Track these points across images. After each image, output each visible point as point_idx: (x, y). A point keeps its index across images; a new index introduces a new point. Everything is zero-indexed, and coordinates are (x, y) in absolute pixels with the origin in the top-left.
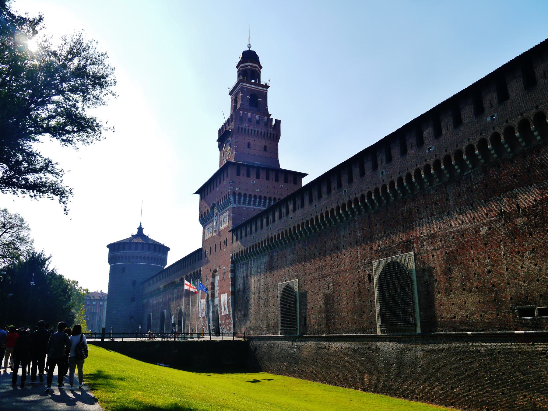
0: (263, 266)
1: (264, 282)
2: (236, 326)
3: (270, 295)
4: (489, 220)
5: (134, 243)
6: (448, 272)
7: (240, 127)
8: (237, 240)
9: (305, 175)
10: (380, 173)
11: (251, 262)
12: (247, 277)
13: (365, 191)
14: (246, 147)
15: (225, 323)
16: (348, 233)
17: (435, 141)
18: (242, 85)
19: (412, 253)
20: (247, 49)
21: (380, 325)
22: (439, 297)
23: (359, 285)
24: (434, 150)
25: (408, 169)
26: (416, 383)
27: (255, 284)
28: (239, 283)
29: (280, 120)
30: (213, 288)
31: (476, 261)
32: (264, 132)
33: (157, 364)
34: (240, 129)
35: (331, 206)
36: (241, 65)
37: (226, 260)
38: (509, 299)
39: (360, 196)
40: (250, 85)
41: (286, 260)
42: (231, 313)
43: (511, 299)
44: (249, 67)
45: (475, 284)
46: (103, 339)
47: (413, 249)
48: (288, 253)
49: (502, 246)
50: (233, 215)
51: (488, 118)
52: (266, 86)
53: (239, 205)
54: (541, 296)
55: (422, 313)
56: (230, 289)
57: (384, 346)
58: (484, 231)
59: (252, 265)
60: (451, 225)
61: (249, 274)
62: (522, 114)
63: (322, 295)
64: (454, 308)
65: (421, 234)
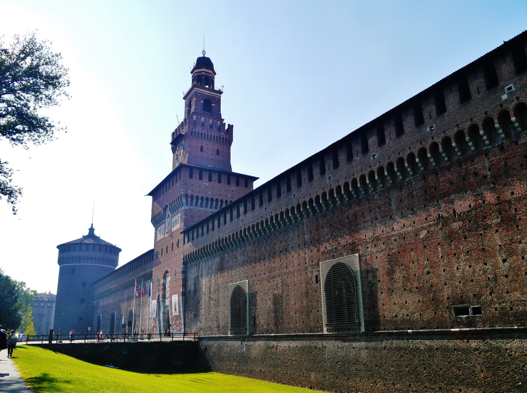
0: (214, 267)
2: (187, 326)
3: (220, 295)
4: (428, 224)
5: (85, 244)
6: (391, 273)
7: (194, 131)
8: (188, 242)
9: (256, 179)
10: (328, 178)
11: (202, 263)
12: (198, 278)
13: (313, 195)
14: (199, 150)
15: (175, 324)
16: (296, 235)
17: (379, 149)
18: (196, 90)
19: (357, 255)
20: (202, 56)
21: (326, 324)
22: (382, 297)
23: (307, 285)
24: (378, 157)
25: (353, 175)
26: (360, 380)
27: (206, 284)
28: (190, 283)
30: (164, 289)
31: (416, 263)
32: (217, 137)
33: (105, 366)
34: (194, 133)
35: (281, 209)
36: (196, 71)
37: (178, 261)
38: (446, 299)
39: (308, 199)
40: (204, 91)
41: (237, 261)
42: (182, 313)
43: (448, 298)
44: (203, 73)
45: (415, 284)
46: (50, 340)
47: (358, 251)
48: (239, 256)
49: (440, 249)
51: (427, 129)
52: (220, 92)
54: (475, 295)
55: (365, 312)
56: (181, 289)
57: (331, 345)
58: (423, 234)
59: (204, 266)
60: (393, 228)
61: (200, 275)
62: (458, 126)
63: (271, 296)
64: (396, 307)
65: (366, 237)
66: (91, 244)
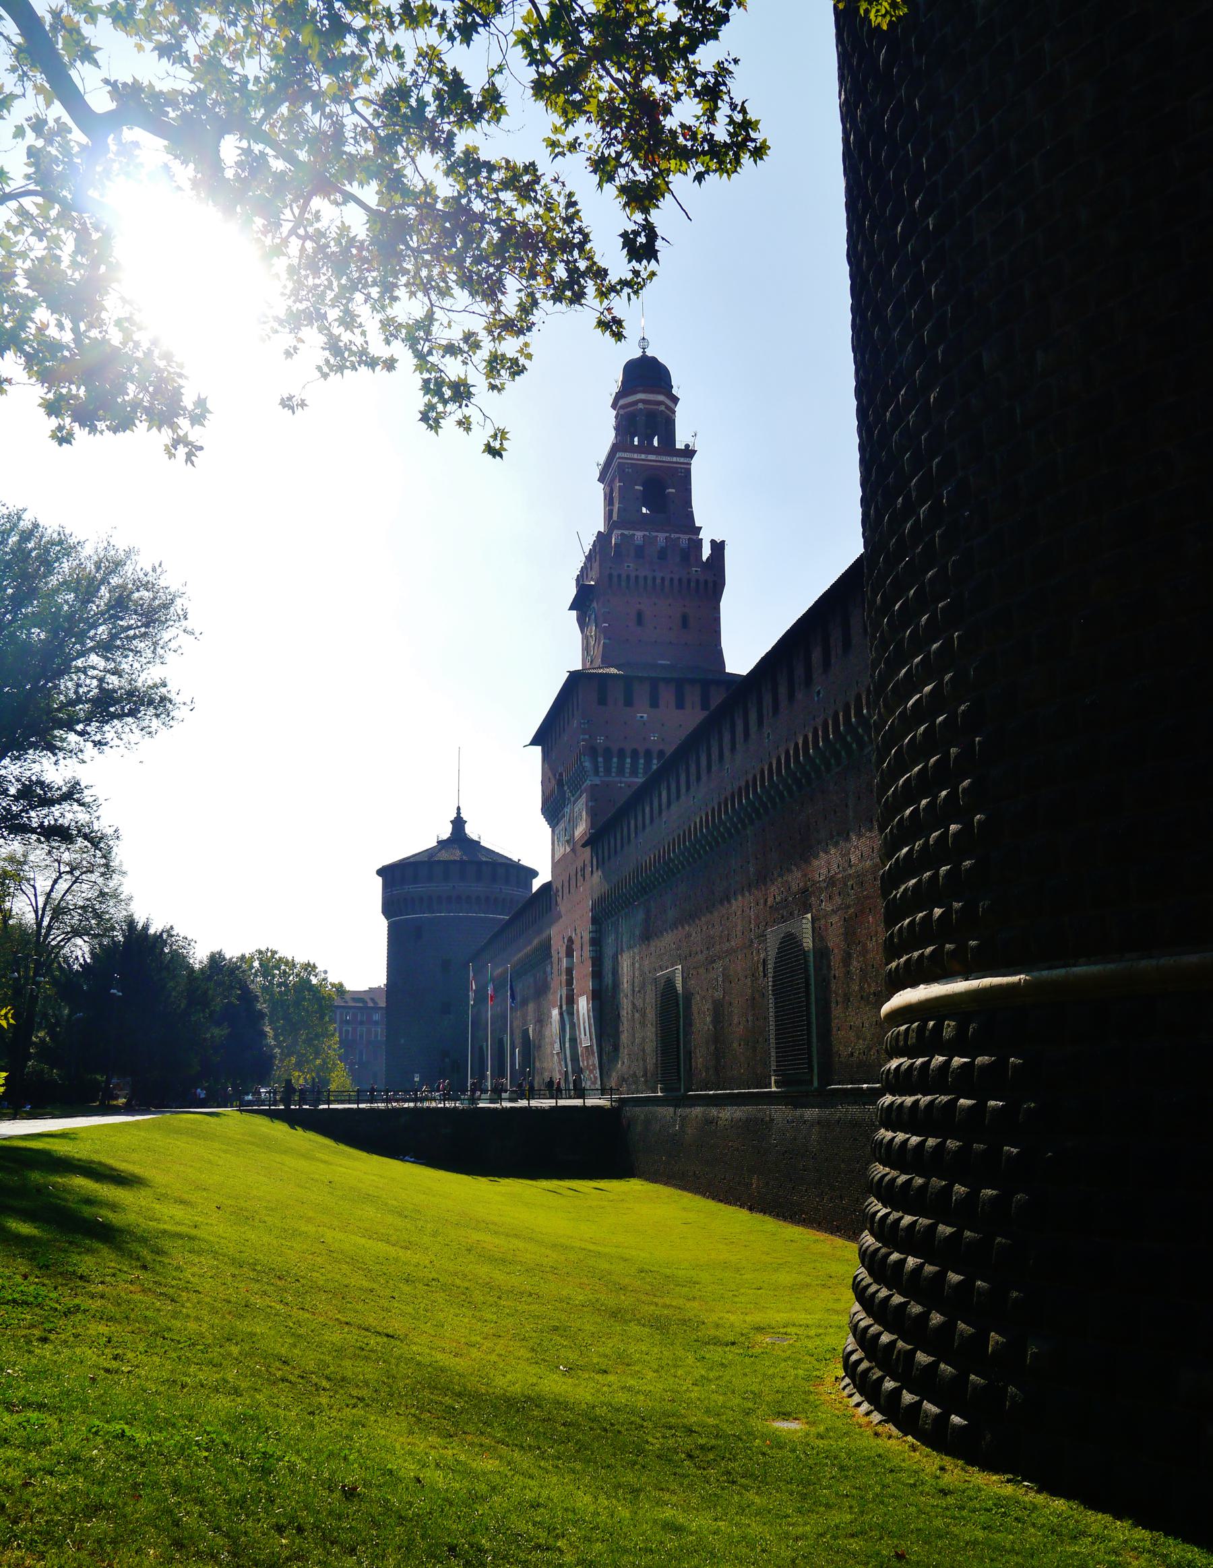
1: (640, 969)
5: (439, 862)
6: (847, 960)
7: (615, 573)
18: (619, 458)
19: (809, 916)
22: (837, 1011)
26: (806, 1191)
29: (724, 541)
32: (680, 580)
33: (402, 1160)
34: (615, 579)
36: (621, 402)
40: (643, 456)
44: (641, 406)
46: (287, 1106)
50: (593, 804)
52: (689, 453)
53: (606, 779)
57: (779, 1113)
66: (455, 862)
